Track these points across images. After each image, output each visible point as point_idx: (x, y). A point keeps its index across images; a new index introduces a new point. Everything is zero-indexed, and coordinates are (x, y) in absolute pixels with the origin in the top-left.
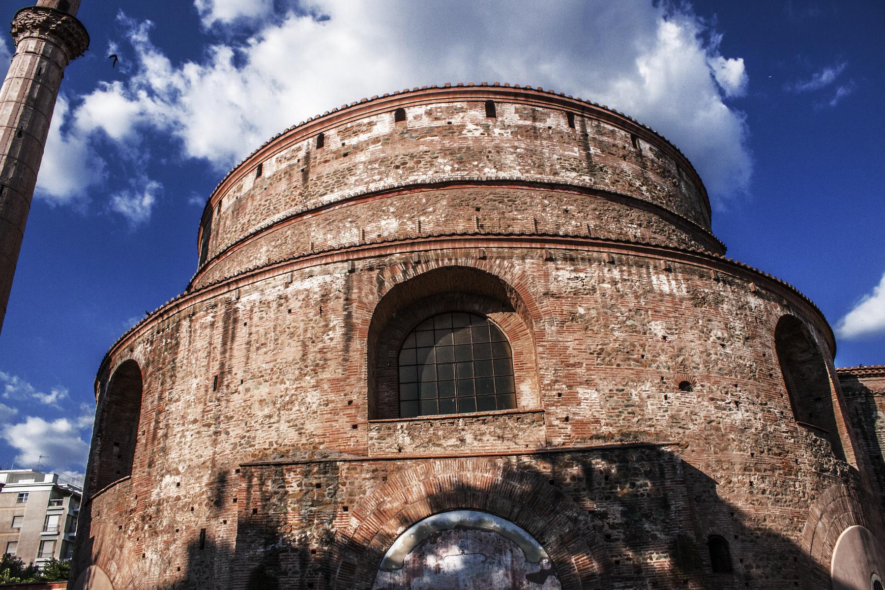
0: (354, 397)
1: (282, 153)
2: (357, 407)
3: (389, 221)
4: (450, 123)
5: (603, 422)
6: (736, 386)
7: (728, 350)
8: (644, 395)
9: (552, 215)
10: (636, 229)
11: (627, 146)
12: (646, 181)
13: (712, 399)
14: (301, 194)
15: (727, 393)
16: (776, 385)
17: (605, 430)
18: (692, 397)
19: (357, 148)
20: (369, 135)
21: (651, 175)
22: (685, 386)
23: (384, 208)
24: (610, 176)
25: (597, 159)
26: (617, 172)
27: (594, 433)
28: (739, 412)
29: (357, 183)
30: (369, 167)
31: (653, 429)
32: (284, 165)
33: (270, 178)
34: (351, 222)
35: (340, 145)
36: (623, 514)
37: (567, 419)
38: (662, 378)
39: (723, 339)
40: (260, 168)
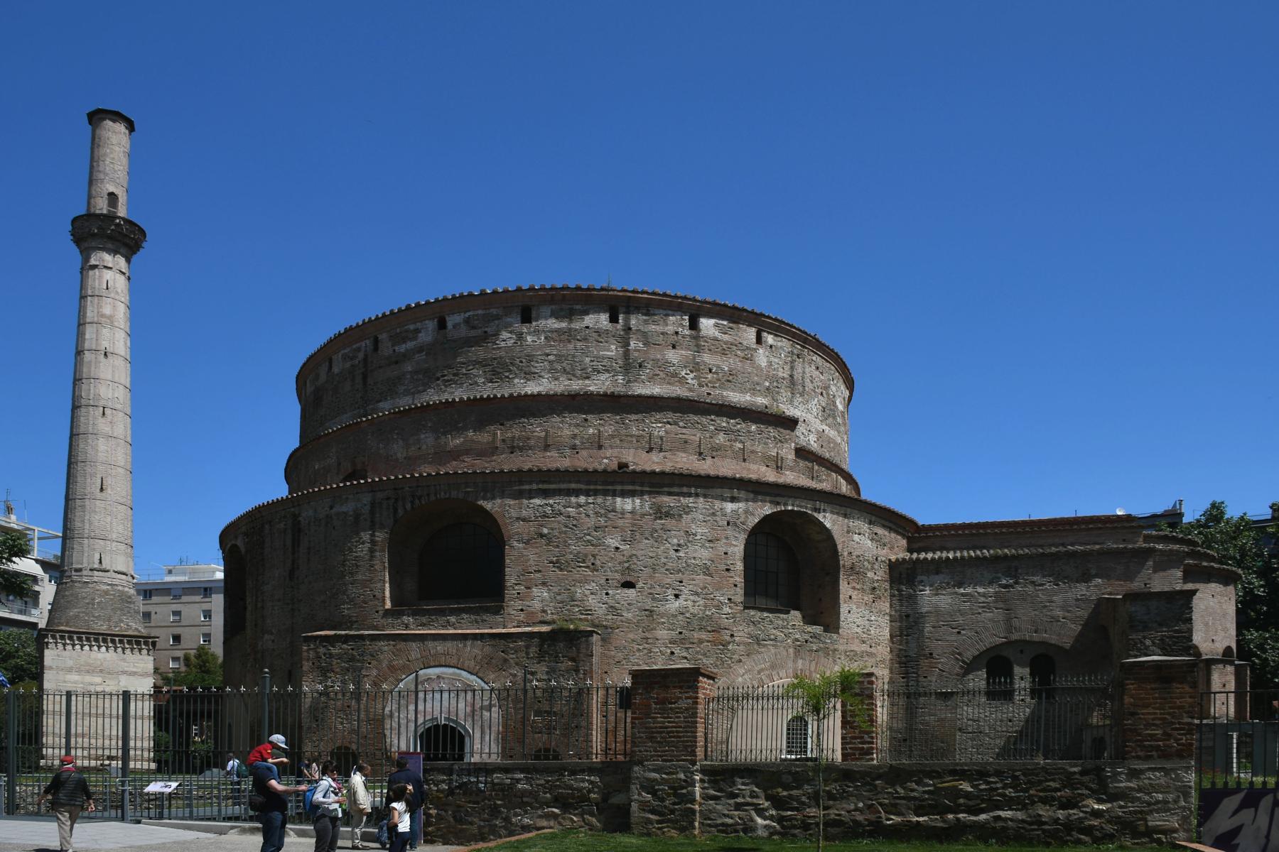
0: (377, 594)
1: (346, 351)
2: (378, 599)
3: (427, 435)
4: (486, 332)
5: (549, 612)
6: (681, 582)
7: (681, 554)
8: (587, 592)
9: (570, 425)
10: (661, 427)
11: (680, 329)
12: (696, 367)
13: (650, 594)
14: (361, 397)
15: (667, 588)
16: (732, 577)
17: (549, 618)
18: (631, 593)
19: (406, 356)
20: (414, 343)
21: (707, 358)
22: (629, 585)
23: (423, 423)
24: (648, 371)
25: (636, 354)
26: (660, 364)
27: (542, 619)
28: (677, 604)
29: (407, 393)
30: (415, 377)
31: (589, 617)
32: (348, 365)
33: (337, 374)
34: (397, 434)
35: (391, 352)
36: (548, 673)
37: (522, 610)
38: (607, 580)
39: (679, 545)
40: (331, 361)
